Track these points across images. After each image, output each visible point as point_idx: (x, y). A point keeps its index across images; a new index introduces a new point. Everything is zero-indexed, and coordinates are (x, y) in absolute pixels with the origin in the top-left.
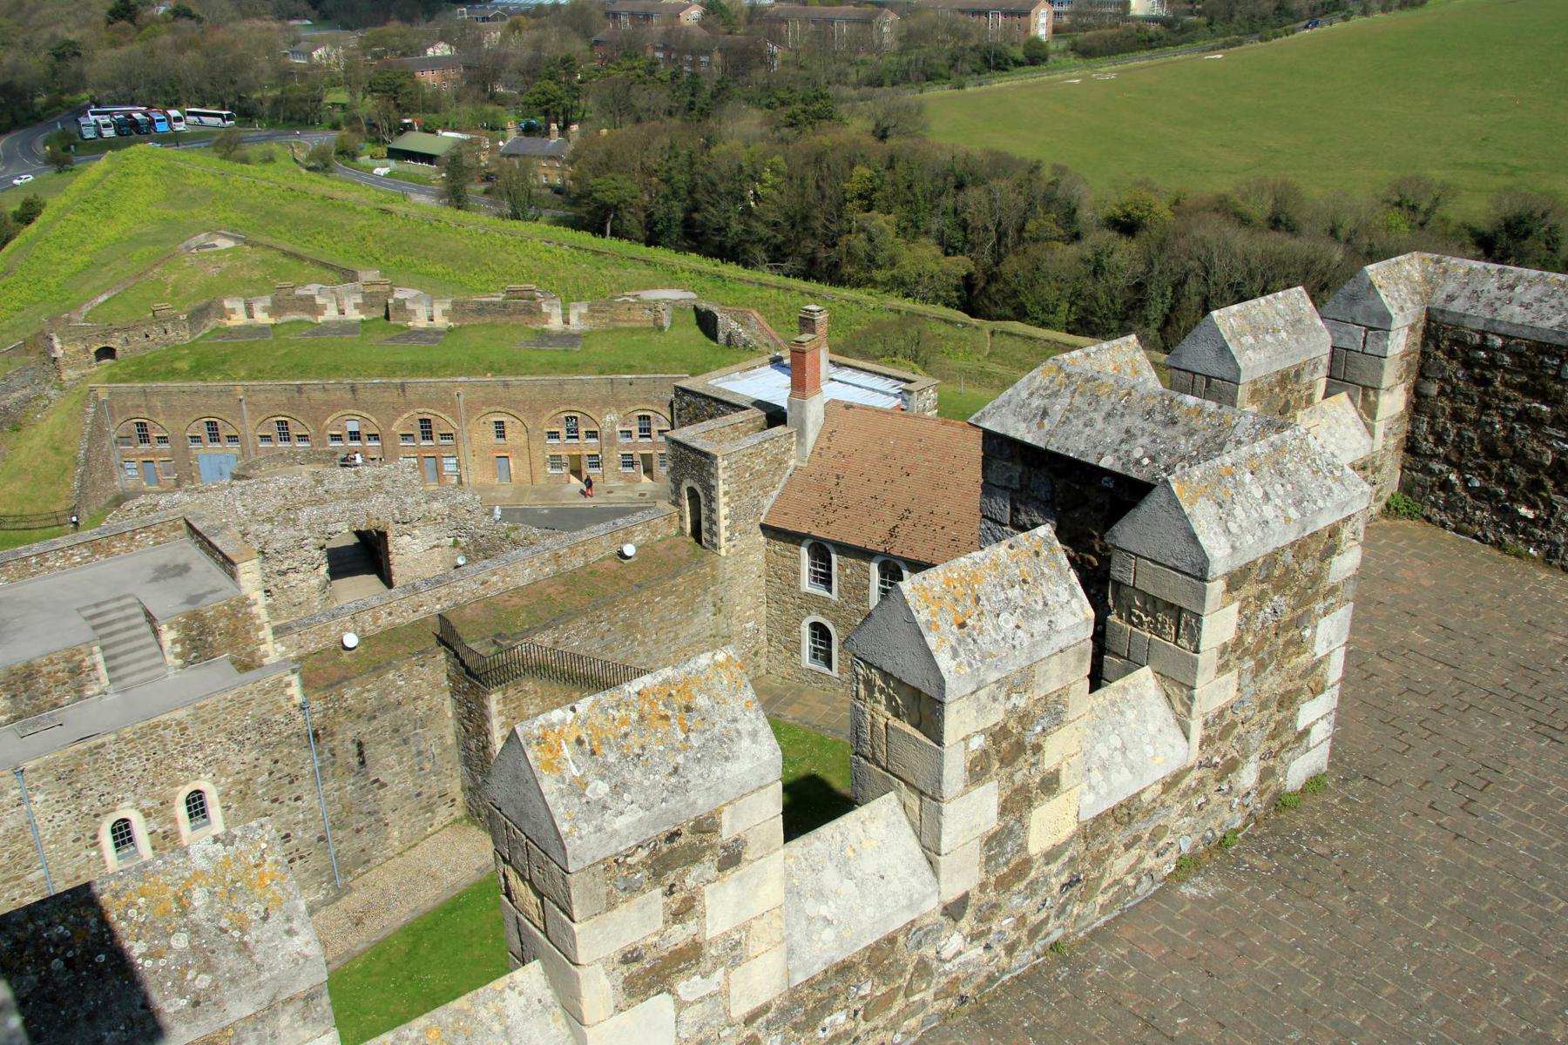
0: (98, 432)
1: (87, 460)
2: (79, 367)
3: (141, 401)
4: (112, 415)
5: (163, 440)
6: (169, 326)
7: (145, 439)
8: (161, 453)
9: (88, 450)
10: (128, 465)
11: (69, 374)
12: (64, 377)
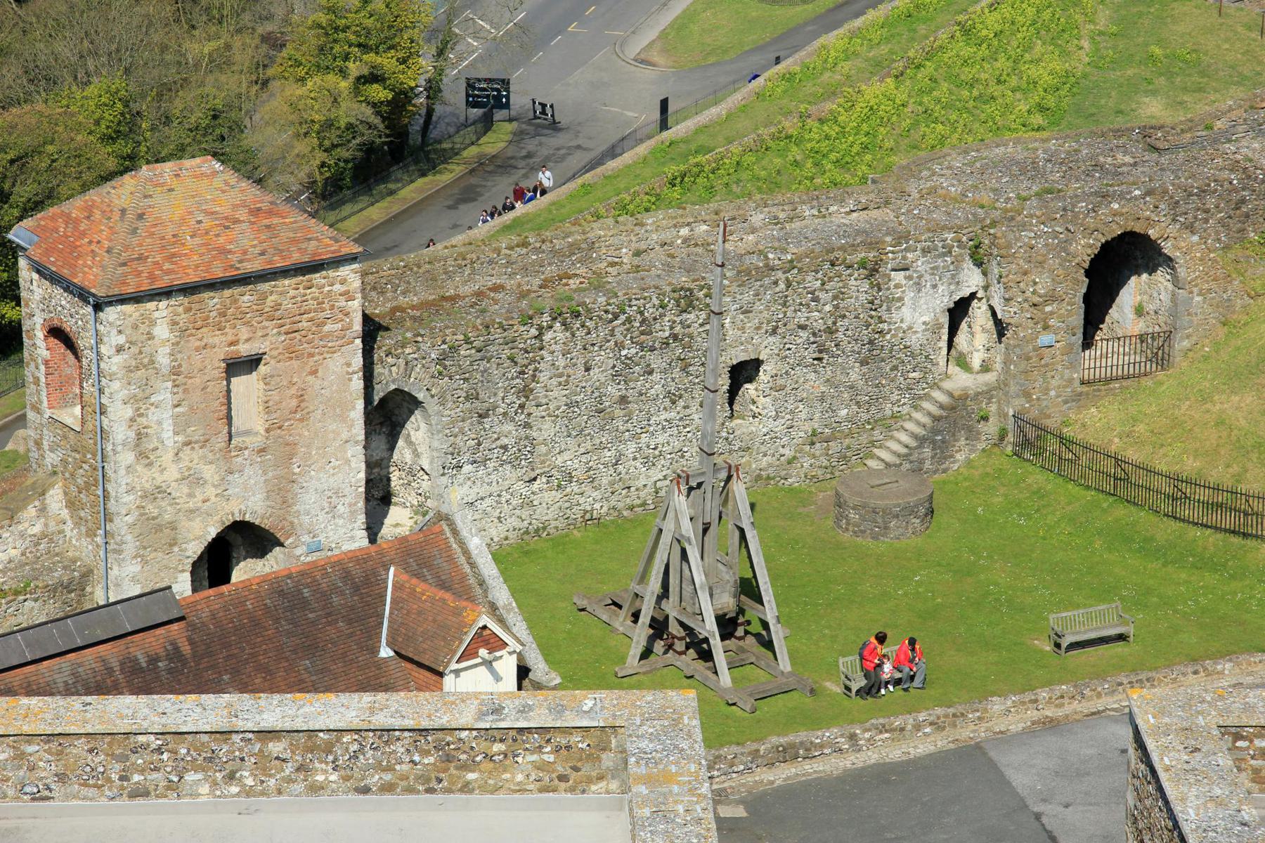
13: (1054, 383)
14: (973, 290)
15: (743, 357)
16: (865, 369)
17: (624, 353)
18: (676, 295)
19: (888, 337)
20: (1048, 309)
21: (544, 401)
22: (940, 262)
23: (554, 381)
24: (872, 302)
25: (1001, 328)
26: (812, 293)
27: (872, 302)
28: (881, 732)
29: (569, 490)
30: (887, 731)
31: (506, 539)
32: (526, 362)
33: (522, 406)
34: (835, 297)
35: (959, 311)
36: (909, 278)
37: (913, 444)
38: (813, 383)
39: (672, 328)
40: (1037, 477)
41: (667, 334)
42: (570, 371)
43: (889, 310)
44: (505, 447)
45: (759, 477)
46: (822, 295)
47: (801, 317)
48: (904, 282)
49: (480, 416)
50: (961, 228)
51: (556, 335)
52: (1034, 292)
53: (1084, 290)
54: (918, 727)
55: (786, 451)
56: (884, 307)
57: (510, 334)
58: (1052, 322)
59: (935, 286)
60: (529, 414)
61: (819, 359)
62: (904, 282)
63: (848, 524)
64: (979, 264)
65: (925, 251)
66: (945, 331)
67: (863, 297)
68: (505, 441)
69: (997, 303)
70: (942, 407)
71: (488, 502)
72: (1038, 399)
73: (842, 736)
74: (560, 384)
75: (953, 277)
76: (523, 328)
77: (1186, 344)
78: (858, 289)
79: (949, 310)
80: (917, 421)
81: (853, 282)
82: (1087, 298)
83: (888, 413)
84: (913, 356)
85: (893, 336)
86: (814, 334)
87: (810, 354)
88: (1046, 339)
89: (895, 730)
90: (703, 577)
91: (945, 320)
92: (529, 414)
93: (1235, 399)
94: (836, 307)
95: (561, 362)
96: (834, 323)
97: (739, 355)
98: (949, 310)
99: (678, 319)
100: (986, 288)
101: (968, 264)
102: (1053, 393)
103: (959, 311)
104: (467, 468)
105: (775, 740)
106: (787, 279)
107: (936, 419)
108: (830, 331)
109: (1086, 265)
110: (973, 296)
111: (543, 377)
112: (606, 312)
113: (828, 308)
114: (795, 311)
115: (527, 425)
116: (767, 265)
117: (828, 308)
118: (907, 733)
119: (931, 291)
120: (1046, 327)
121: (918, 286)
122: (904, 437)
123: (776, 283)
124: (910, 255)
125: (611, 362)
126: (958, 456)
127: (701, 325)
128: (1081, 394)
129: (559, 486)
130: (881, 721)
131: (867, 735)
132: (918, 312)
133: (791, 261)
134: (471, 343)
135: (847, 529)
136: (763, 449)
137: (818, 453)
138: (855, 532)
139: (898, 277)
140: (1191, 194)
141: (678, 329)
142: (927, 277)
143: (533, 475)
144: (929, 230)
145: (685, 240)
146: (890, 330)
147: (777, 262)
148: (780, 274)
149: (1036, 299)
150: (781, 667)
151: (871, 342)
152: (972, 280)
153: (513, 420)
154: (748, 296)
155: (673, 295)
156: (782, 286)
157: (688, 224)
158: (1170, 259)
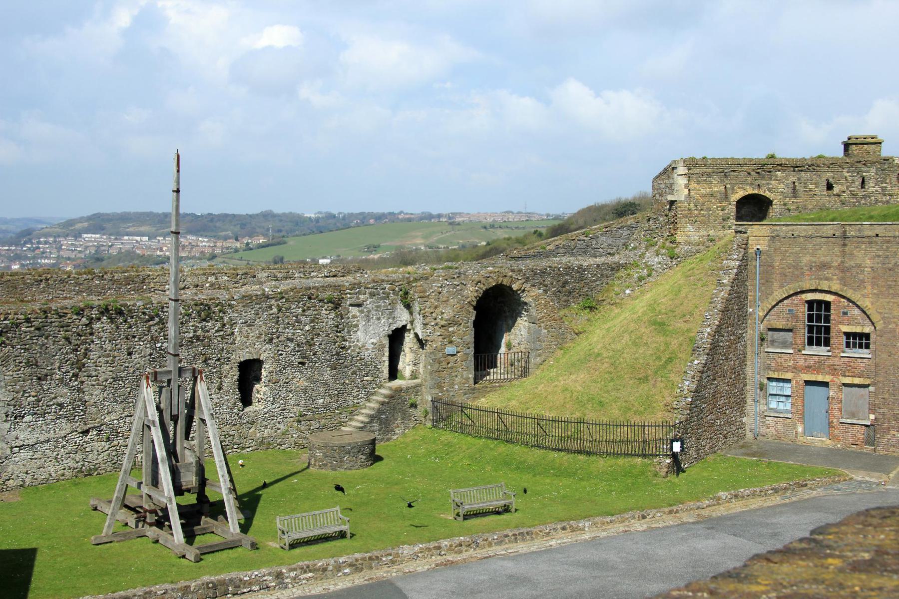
0: (734, 311)
1: (714, 346)
2: (705, 224)
3: (830, 254)
4: (767, 281)
5: (859, 340)
6: (871, 174)
7: (819, 334)
8: (848, 368)
9: (718, 331)
10: (773, 387)
11: (688, 233)
12: (680, 237)
13: (457, 380)
14: (404, 323)
15: (248, 357)
16: (334, 372)
17: (159, 345)
18: (198, 308)
19: (349, 351)
20: (451, 329)
21: (94, 374)
22: (382, 303)
23: (102, 360)
24: (337, 326)
25: (422, 343)
26: (296, 317)
27: (337, 326)
28: (305, 572)
29: (116, 442)
30: (310, 571)
31: (63, 475)
32: (79, 342)
33: (76, 376)
34: (312, 321)
35: (396, 338)
36: (362, 312)
37: (367, 420)
38: (300, 380)
39: (195, 331)
40: (447, 436)
41: (191, 335)
42: (116, 354)
43: (349, 332)
44: (61, 405)
45: (262, 443)
46: (303, 319)
47: (289, 332)
48: (358, 314)
49: (39, 379)
50: (394, 281)
51: (103, 325)
52: (442, 319)
53: (473, 318)
54: (338, 568)
55: (281, 426)
56: (346, 330)
57: (66, 320)
58: (454, 339)
59: (379, 319)
60: (82, 382)
61: (303, 364)
62: (358, 314)
63: (315, 461)
64: (408, 307)
65: (372, 295)
66: (387, 349)
67: (331, 322)
68: (61, 400)
69: (419, 331)
70: (385, 396)
71: (46, 446)
72: (447, 390)
73: (269, 574)
74: (107, 362)
75: (391, 313)
76: (75, 317)
77: (538, 360)
78: (328, 317)
79: (389, 336)
80: (370, 407)
81: (324, 312)
82: (476, 324)
83: (351, 403)
84: (366, 365)
85: (352, 351)
86: (298, 345)
87: (296, 359)
88: (450, 349)
89: (318, 570)
90: (164, 453)
91: (386, 342)
92: (82, 382)
93: (573, 377)
94: (313, 328)
95: (108, 346)
96: (313, 339)
97: (245, 356)
98: (389, 336)
99: (199, 325)
100: (412, 322)
101: (400, 307)
102: (456, 387)
103: (396, 338)
104: (28, 418)
105: (206, 578)
106: (278, 305)
107: (383, 403)
108: (310, 344)
109: (474, 303)
110: (404, 327)
111: (92, 355)
112: (144, 313)
113: (307, 328)
114: (285, 328)
115: (80, 390)
116: (264, 294)
117: (307, 328)
118: (329, 573)
119: (377, 322)
120: (451, 342)
121: (368, 318)
122: (360, 418)
123: (270, 307)
124: (362, 297)
125: (148, 351)
126: (397, 431)
127: (217, 331)
128: (474, 389)
129: (108, 439)
130: (306, 562)
131: (292, 574)
132: (369, 336)
133: (281, 293)
134: (31, 322)
135: (315, 465)
136: (264, 423)
137: (303, 428)
138: (320, 466)
139: (354, 311)
140: (536, 274)
141: (199, 332)
142: (374, 312)
143: (85, 428)
144: (374, 281)
145: (212, 285)
146: (350, 347)
147: (270, 293)
148: (273, 302)
149: (443, 323)
150: (232, 530)
151: (338, 354)
152: (403, 317)
153: (67, 385)
154: (251, 314)
155: (194, 307)
156: (275, 310)
157: (214, 274)
158: (526, 304)
